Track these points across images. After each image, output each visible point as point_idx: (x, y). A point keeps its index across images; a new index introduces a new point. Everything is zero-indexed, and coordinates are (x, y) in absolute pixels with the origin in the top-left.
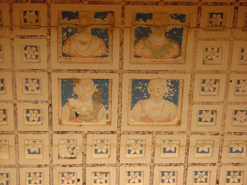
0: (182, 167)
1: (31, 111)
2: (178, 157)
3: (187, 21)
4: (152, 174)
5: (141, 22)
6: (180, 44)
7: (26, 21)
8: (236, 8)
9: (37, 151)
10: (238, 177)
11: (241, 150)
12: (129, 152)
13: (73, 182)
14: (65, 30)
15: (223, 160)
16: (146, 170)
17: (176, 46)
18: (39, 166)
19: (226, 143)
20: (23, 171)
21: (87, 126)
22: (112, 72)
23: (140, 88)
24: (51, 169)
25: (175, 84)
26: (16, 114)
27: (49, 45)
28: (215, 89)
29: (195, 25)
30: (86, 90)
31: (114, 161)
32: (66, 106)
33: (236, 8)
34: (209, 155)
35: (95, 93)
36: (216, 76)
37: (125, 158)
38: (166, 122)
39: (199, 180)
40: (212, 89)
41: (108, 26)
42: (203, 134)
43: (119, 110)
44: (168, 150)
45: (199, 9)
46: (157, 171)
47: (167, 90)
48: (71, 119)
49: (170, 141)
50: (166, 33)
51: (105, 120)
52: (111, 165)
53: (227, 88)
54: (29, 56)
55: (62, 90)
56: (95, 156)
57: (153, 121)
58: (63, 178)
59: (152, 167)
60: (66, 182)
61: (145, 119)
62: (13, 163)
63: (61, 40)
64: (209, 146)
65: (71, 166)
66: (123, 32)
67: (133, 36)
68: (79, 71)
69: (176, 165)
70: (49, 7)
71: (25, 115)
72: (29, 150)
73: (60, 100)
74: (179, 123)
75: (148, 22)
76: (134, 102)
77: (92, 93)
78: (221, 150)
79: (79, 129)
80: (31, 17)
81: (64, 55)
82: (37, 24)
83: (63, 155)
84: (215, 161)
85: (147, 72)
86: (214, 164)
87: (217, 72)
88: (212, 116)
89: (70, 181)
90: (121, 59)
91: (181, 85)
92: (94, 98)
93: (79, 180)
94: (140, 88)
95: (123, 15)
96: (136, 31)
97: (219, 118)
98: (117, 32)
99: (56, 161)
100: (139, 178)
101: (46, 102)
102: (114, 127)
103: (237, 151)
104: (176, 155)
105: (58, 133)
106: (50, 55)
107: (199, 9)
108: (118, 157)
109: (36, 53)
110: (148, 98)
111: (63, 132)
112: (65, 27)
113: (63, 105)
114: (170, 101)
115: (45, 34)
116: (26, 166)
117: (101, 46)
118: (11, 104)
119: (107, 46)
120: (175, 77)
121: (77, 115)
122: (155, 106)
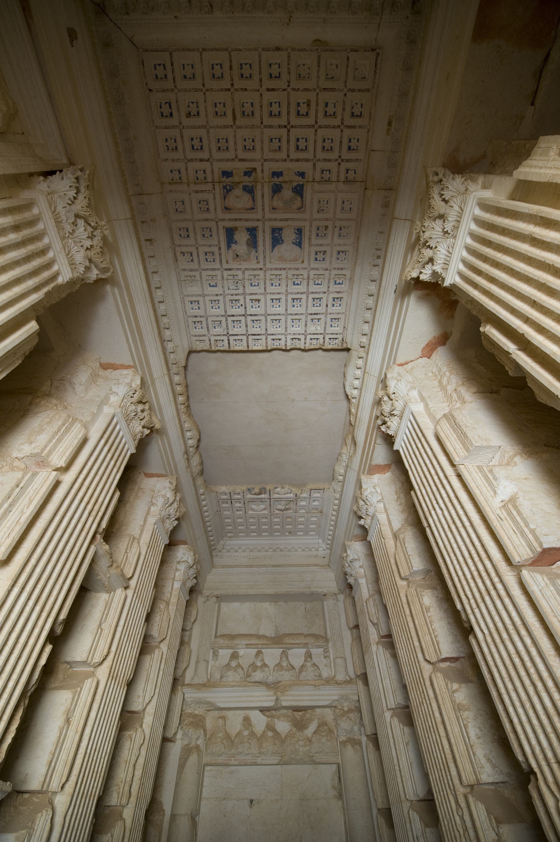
0: (305, 295)
1: (208, 254)
2: (302, 288)
3: (306, 178)
4: (287, 300)
5: (276, 179)
6: (302, 198)
7: (197, 179)
8: (339, 164)
9: (215, 285)
10: (340, 303)
11: (341, 282)
12: (272, 284)
13: (239, 307)
14: (225, 187)
15: (330, 290)
16: (283, 297)
17: (299, 199)
18: (217, 295)
19: (332, 276)
20: (208, 299)
21: (244, 265)
22: (258, 220)
23: (277, 235)
24: (224, 297)
25: (299, 231)
26: (198, 256)
27: (215, 199)
28: (325, 234)
29: (311, 179)
30: (242, 237)
31: (263, 291)
32: (230, 249)
33: (339, 164)
34: (322, 286)
35: (248, 239)
36: (326, 223)
37: (270, 289)
38: (294, 261)
39: (316, 305)
40: (323, 235)
41: (253, 183)
42: (317, 269)
43: (264, 252)
44: (296, 283)
45: (314, 165)
46: (290, 297)
47: (294, 236)
48: (234, 259)
49: (297, 275)
50: (293, 189)
51: (255, 261)
52: (261, 294)
53: (333, 233)
54: (202, 209)
55: (227, 236)
56: (251, 288)
57: (286, 260)
58: (233, 305)
59: (286, 295)
60: (234, 307)
61: (281, 259)
62: (201, 293)
63: (223, 195)
64: (322, 280)
65: (236, 295)
66: (263, 186)
67: (271, 191)
68: (236, 220)
69: (302, 293)
70: (212, 165)
71: (205, 257)
72: (210, 284)
73: (226, 245)
74: (303, 262)
75: (281, 179)
76: (274, 246)
77: (246, 239)
78: (329, 282)
79: (239, 267)
80: (201, 175)
81: (226, 208)
82: (205, 181)
83: (231, 288)
84: (326, 290)
85: (281, 220)
86: (325, 293)
87: (327, 219)
88: (323, 256)
89: (237, 307)
90: (263, 209)
91: (303, 232)
92: (248, 244)
93: (242, 305)
94: (277, 235)
95: (262, 170)
96: (272, 186)
97: (328, 257)
98: (259, 186)
99: (227, 292)
100: (279, 304)
101: (217, 246)
102: (261, 265)
103: (339, 284)
104: (301, 286)
105: (226, 270)
106: (216, 207)
107: (314, 165)
108: (265, 288)
109: (207, 207)
110: (283, 243)
111: (230, 269)
112: (225, 184)
113: (228, 250)
114: (297, 245)
115: (211, 189)
116: (208, 295)
117: (249, 199)
118: (195, 248)
119: (254, 201)
120: (299, 224)
121: (237, 256)
122: (287, 248)
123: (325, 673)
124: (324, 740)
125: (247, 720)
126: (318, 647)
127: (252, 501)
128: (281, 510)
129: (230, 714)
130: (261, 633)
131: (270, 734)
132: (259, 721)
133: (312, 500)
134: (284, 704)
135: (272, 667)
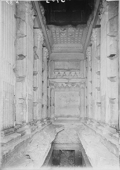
123: (79, 77)
124: (77, 88)
125: (62, 84)
126: (78, 72)
127: (62, 32)
128: (70, 35)
129: (59, 83)
130: (65, 69)
131: (67, 87)
132: (65, 85)
133: (79, 32)
134: (70, 82)
135: (67, 75)
